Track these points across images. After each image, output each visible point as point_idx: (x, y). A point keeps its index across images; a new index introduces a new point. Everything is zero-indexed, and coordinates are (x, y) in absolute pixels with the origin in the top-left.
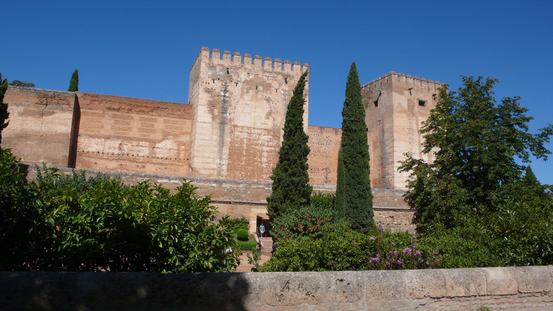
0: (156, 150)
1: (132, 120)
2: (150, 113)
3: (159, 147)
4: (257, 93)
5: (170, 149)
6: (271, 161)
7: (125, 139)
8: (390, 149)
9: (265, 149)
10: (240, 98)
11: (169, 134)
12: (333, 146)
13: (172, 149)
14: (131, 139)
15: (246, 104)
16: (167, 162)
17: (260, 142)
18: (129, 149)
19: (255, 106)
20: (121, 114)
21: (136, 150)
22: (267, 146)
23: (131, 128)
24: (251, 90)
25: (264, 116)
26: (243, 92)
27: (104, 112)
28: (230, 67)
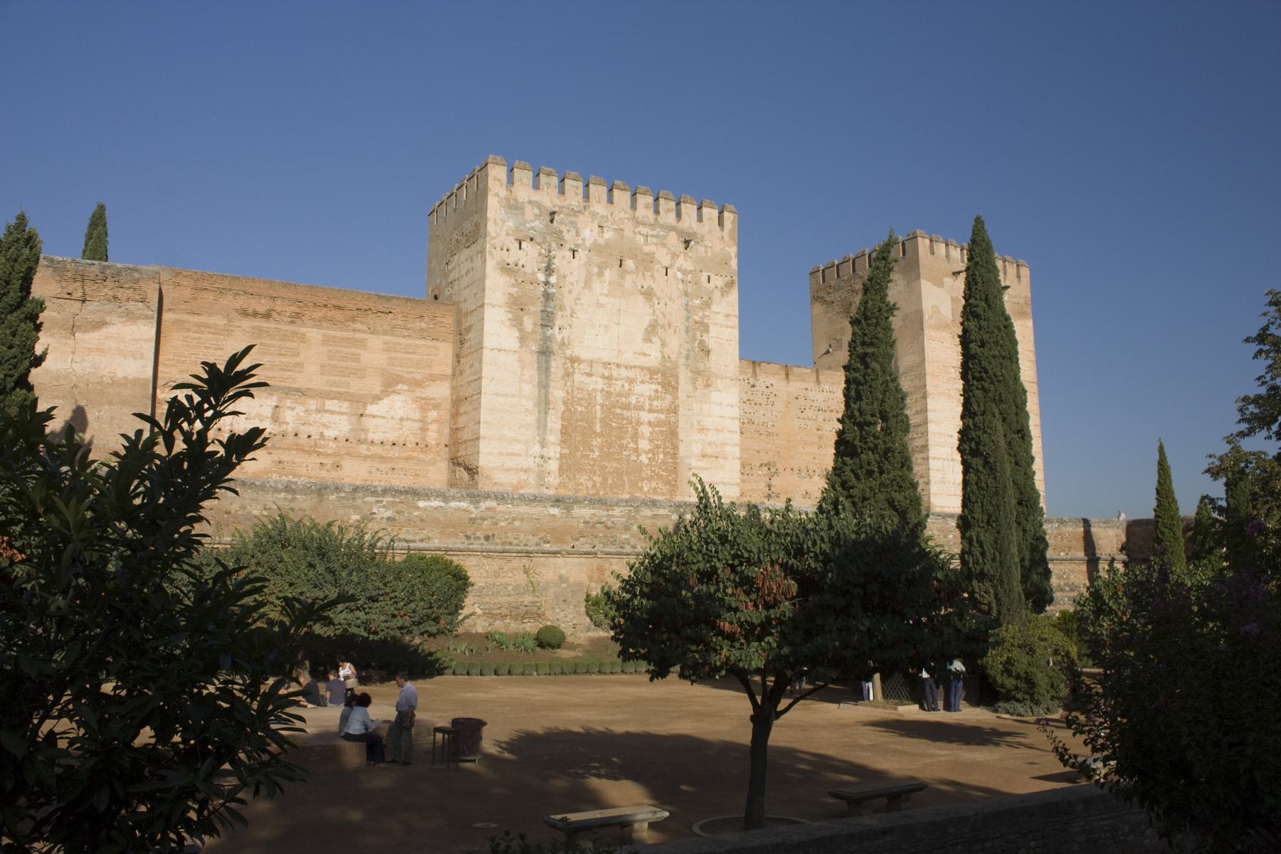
0: (368, 422)
1: (305, 342)
2: (350, 323)
3: (375, 413)
4: (622, 277)
5: (401, 419)
6: (658, 447)
7: (287, 394)
8: (918, 416)
9: (646, 417)
10: (584, 288)
11: (398, 379)
12: (783, 410)
13: (408, 419)
14: (303, 393)
15: (599, 305)
16: (395, 453)
17: (633, 400)
18: (298, 420)
19: (619, 310)
20: (273, 326)
21: (315, 423)
22: (650, 411)
23: (303, 364)
24: (608, 269)
25: (640, 335)
26: (589, 275)
27: (229, 321)
28: (556, 209)
